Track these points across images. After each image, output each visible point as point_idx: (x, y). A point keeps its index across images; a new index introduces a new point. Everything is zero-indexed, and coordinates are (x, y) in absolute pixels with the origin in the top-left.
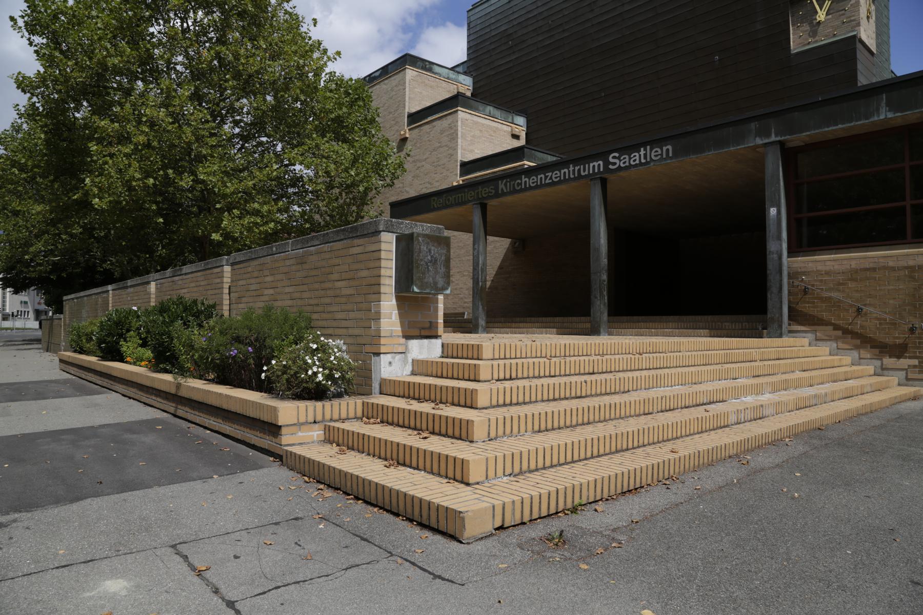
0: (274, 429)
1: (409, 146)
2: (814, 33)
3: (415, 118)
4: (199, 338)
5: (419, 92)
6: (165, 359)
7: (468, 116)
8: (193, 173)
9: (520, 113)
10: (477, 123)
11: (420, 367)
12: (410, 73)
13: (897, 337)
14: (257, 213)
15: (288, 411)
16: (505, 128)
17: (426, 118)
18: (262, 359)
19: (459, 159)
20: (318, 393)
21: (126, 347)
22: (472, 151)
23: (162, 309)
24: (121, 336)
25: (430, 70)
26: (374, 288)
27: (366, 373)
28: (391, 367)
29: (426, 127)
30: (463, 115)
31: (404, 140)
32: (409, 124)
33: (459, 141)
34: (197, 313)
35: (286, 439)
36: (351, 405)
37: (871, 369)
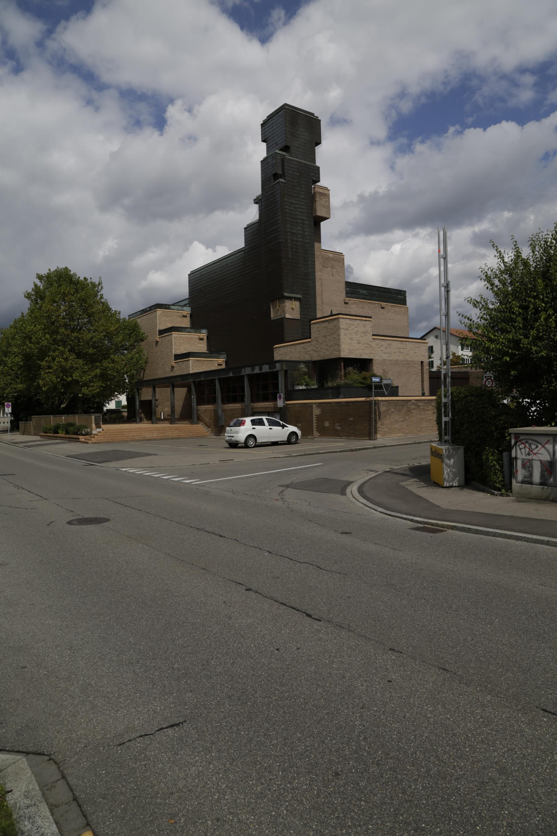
0: (79, 439)
1: (159, 344)
2: (277, 313)
3: (161, 332)
4: (72, 429)
5: (163, 320)
6: (67, 432)
7: (177, 335)
8: (72, 377)
9: (203, 328)
10: (181, 337)
11: (99, 432)
12: (159, 312)
13: (209, 424)
14: (93, 386)
15: (80, 437)
16: (196, 336)
17: (164, 334)
18: (79, 431)
19: (174, 353)
20: (84, 435)
21: (59, 431)
22: (180, 349)
23: (66, 424)
24: (59, 429)
25: (169, 309)
26: (91, 423)
27: (91, 433)
28: (94, 432)
29: (164, 338)
30: (175, 334)
31: (157, 342)
32: (160, 335)
33: (173, 346)
34: (72, 425)
35: (81, 440)
36: (87, 437)
37: (206, 431)
